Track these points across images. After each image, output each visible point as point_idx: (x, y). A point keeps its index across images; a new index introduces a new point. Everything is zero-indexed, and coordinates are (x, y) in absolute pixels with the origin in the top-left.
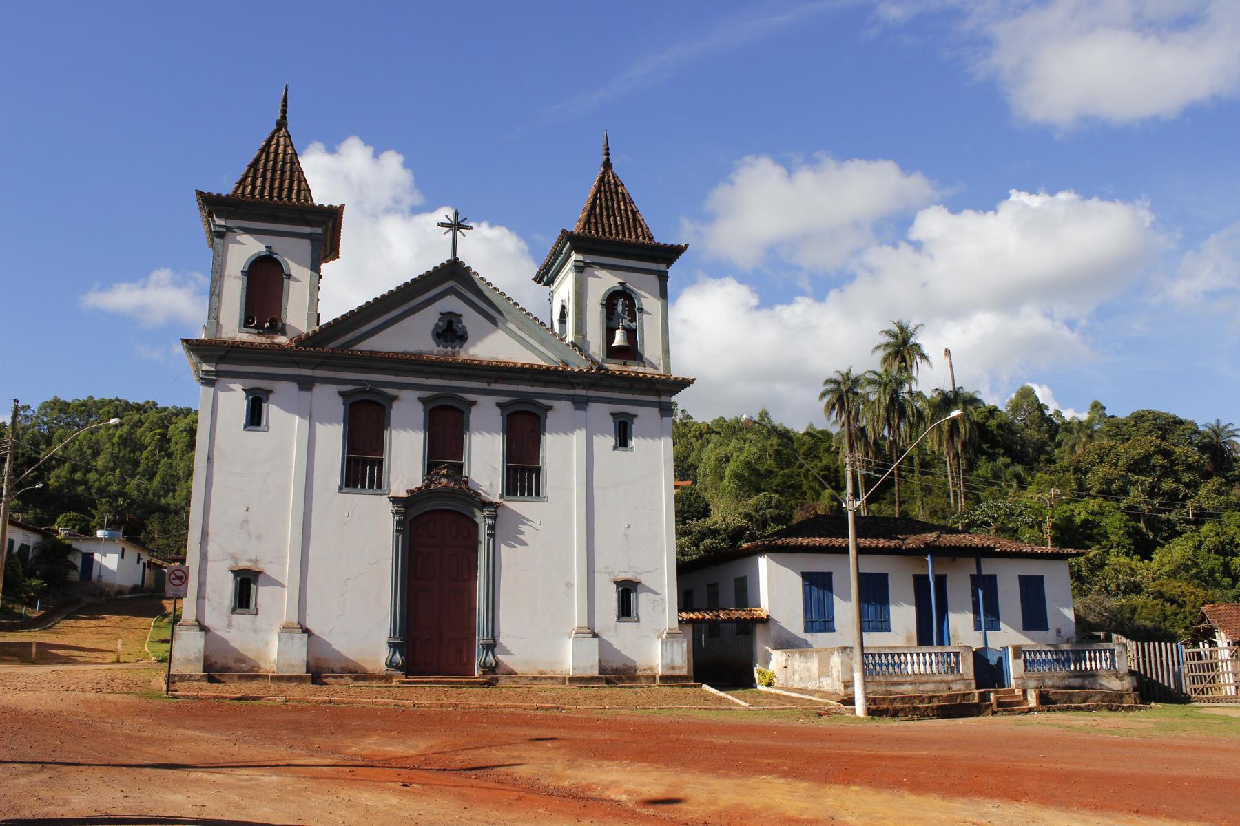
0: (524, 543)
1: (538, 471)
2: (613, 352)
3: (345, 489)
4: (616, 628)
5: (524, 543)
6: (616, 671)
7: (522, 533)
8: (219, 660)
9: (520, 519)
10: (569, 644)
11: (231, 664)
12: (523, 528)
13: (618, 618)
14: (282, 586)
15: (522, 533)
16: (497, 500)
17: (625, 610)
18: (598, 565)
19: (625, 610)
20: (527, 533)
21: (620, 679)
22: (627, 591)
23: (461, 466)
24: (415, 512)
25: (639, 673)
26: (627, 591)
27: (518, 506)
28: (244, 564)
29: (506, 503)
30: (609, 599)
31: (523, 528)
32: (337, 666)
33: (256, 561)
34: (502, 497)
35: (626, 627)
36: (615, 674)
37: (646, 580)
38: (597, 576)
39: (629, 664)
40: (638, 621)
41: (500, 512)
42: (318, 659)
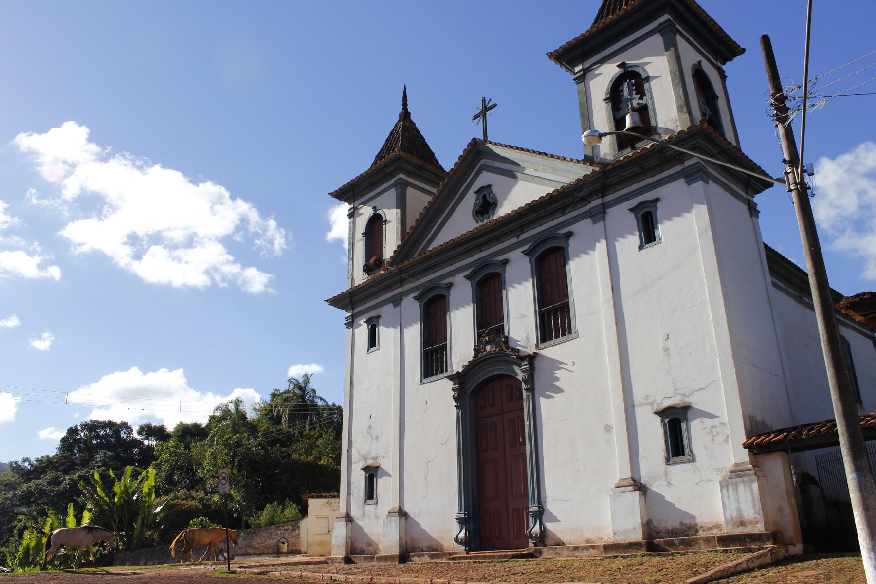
0: (560, 390)
1: (567, 306)
2: (623, 141)
3: (424, 381)
4: (666, 474)
5: (560, 390)
6: (673, 533)
7: (557, 379)
8: (360, 545)
9: (555, 364)
10: (607, 501)
11: (365, 548)
12: (558, 374)
13: (667, 460)
14: (390, 476)
15: (557, 379)
16: (531, 350)
17: (677, 447)
18: (638, 395)
19: (677, 447)
20: (563, 377)
21: (671, 544)
22: (675, 421)
23: (501, 329)
24: (471, 386)
25: (702, 534)
26: (675, 421)
27: (553, 351)
28: (370, 462)
29: (543, 352)
30: (653, 434)
31: (558, 374)
32: (424, 544)
33: (375, 459)
34: (537, 346)
35: (680, 470)
36: (664, 537)
37: (697, 402)
38: (638, 411)
39: (688, 522)
40: (693, 460)
41: (537, 363)
42: (412, 540)
